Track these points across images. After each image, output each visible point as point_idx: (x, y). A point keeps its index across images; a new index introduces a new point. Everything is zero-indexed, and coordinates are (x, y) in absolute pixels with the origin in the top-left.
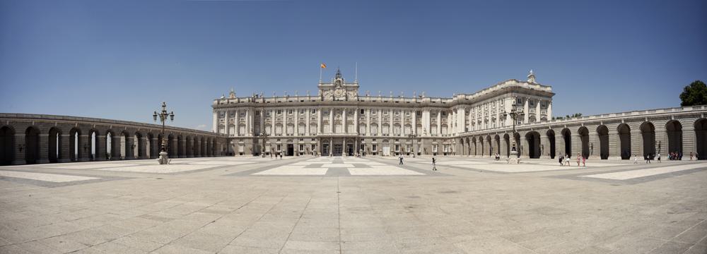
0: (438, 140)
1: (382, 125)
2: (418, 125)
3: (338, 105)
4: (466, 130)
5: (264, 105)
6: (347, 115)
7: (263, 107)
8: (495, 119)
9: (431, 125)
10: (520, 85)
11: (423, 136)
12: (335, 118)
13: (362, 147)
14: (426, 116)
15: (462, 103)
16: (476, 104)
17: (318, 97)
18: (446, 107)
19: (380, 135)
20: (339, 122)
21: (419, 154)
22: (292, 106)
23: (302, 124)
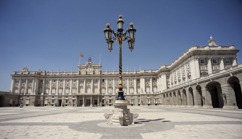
0: (151, 96)
1: (115, 88)
2: (138, 87)
3: (89, 77)
4: (168, 88)
5: (45, 76)
6: (94, 83)
7: (45, 77)
8: (185, 78)
9: (146, 87)
10: (201, 49)
11: (141, 93)
12: (87, 85)
13: (103, 101)
14: (142, 81)
15: (164, 71)
16: (173, 70)
17: (77, 72)
18: (155, 75)
19: (114, 94)
20: (89, 87)
21: (139, 105)
22: (62, 77)
23: (67, 88)
